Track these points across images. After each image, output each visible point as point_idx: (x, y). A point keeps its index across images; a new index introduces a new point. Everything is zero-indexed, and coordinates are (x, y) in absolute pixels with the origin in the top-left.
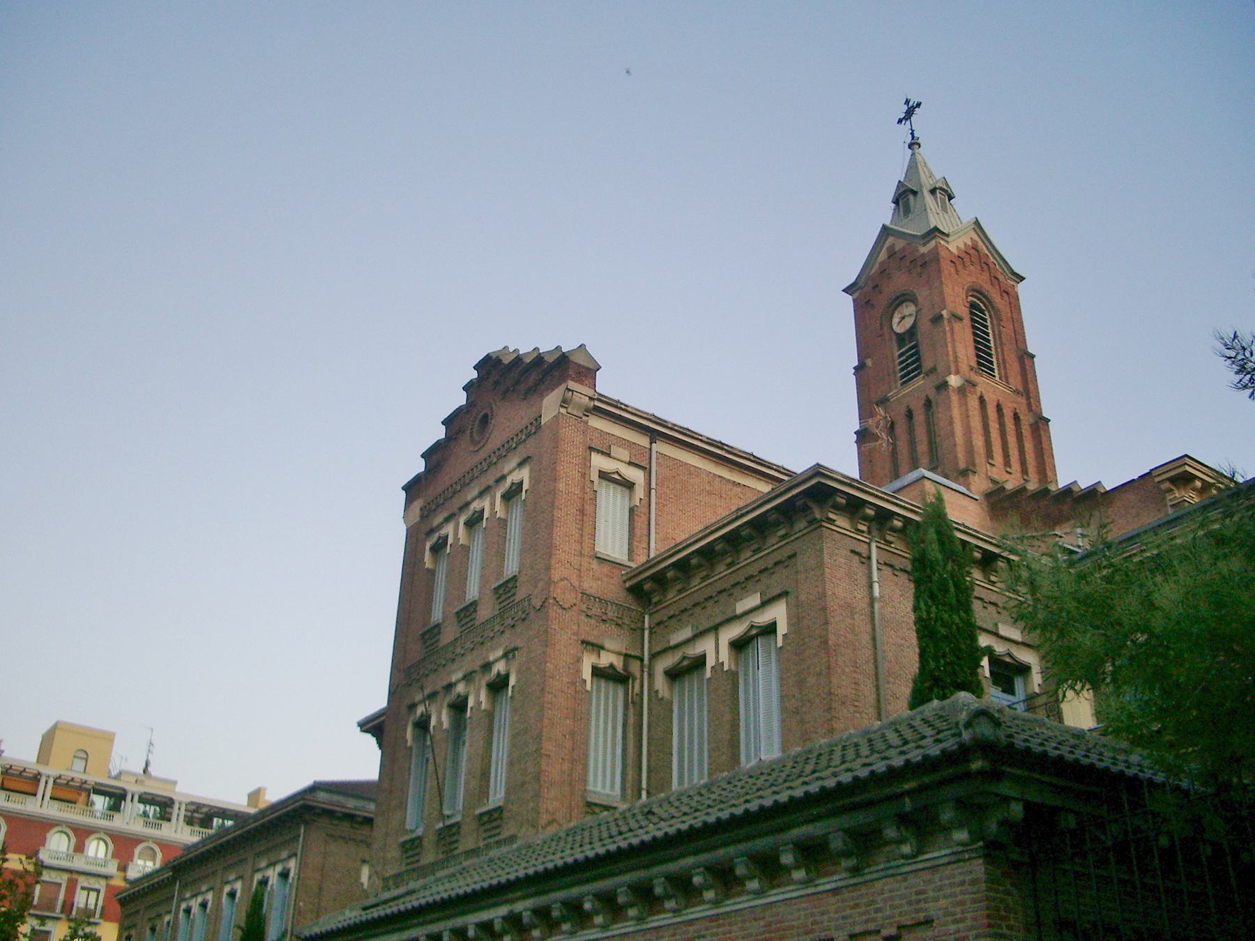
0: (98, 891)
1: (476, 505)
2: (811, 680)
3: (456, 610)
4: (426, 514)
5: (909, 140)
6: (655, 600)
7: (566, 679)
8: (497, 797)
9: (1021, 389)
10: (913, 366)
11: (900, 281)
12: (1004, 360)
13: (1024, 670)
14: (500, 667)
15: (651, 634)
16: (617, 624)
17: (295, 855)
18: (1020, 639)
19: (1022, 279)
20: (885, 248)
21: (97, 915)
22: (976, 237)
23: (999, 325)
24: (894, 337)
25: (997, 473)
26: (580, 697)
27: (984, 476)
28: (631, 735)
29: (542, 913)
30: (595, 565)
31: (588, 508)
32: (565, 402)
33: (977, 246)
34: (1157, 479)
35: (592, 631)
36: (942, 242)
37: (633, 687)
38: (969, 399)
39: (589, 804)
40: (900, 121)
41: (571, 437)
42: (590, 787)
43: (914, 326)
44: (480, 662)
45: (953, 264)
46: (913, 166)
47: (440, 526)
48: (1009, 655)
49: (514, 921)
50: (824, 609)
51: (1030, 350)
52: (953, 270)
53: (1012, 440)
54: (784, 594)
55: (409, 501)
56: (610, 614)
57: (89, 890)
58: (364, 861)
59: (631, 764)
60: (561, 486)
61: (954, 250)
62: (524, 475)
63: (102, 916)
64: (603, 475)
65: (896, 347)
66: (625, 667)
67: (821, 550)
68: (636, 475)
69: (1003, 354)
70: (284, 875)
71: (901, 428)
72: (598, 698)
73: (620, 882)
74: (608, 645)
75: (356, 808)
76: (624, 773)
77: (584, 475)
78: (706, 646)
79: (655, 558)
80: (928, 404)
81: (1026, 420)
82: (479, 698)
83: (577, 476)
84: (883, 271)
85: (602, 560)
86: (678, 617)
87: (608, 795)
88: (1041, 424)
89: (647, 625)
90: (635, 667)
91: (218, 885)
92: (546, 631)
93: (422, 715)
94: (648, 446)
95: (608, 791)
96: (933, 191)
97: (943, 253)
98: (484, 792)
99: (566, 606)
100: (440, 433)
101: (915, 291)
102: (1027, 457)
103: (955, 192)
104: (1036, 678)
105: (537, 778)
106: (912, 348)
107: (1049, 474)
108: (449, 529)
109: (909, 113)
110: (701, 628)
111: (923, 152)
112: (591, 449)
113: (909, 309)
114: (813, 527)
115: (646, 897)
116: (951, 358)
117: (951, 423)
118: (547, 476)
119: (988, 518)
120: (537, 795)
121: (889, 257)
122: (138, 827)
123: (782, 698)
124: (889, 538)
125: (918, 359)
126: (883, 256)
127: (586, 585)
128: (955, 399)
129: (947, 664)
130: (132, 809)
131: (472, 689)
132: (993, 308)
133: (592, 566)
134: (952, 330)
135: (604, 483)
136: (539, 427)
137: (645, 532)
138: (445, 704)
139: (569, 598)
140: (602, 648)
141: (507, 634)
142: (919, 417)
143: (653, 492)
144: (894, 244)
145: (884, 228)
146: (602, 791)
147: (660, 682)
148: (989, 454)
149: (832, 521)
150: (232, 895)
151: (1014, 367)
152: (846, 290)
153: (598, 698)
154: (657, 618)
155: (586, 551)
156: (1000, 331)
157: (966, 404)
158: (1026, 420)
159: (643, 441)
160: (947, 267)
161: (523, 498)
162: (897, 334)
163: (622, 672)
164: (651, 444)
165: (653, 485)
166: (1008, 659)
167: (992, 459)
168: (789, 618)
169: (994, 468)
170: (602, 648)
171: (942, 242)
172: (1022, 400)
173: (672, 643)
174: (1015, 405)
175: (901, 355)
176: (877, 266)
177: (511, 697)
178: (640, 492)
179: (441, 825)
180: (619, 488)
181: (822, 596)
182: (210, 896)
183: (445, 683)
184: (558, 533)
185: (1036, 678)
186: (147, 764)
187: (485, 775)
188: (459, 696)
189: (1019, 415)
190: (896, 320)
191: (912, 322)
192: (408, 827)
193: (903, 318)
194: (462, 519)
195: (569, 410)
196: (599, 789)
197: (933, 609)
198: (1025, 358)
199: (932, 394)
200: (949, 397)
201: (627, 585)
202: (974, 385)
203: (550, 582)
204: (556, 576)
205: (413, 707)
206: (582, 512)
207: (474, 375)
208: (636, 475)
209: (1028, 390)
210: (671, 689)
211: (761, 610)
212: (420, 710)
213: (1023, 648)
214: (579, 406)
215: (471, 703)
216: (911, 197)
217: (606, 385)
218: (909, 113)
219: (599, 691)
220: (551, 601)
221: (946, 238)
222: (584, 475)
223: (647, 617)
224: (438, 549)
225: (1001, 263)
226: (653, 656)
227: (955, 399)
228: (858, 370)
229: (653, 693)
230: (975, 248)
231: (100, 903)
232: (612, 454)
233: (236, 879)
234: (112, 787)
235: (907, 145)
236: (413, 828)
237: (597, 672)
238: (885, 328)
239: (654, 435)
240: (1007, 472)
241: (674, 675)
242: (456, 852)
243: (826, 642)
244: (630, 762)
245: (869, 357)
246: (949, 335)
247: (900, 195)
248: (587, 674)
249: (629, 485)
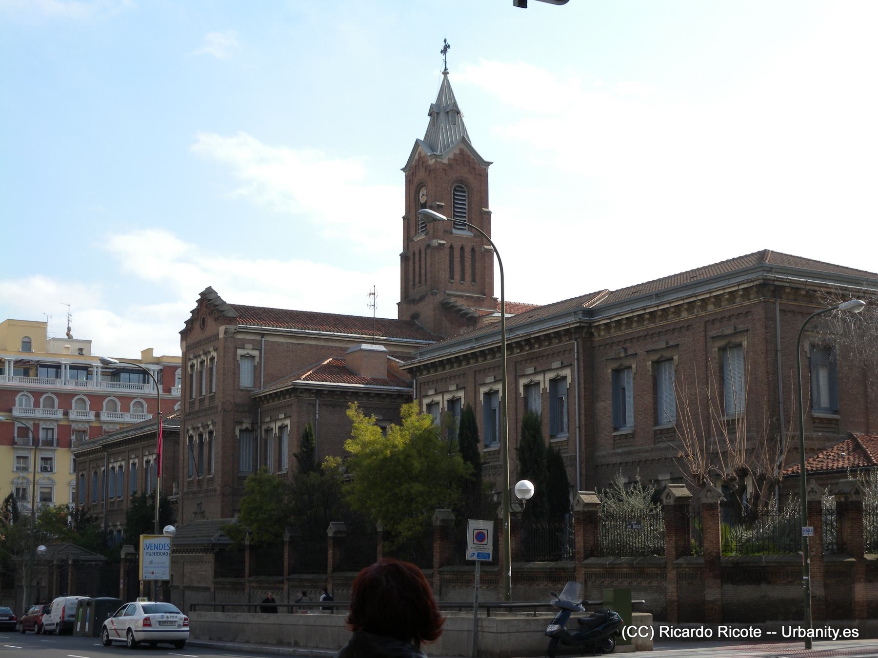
0: (53, 429)
5: (443, 70)
11: (421, 174)
18: (382, 419)
21: (55, 445)
30: (240, 392)
43: (426, 202)
45: (444, 171)
53: (468, 264)
55: (182, 339)
56: (246, 409)
57: (47, 429)
61: (445, 161)
63: (57, 446)
64: (242, 356)
66: (252, 427)
68: (256, 353)
85: (242, 390)
91: (127, 458)
95: (247, 470)
109: (444, 51)
122: (70, 387)
126: (417, 157)
130: (66, 373)
136: (218, 338)
143: (263, 358)
150: (134, 464)
152: (401, 170)
159: (258, 338)
165: (263, 355)
169: (454, 284)
178: (257, 360)
182: (123, 463)
186: (69, 329)
189: (475, 249)
190: (421, 195)
194: (199, 361)
208: (256, 353)
218: (444, 51)
221: (441, 157)
231: (55, 436)
232: (246, 347)
233: (135, 458)
234: (51, 362)
235: (441, 72)
240: (462, 284)
248: (237, 433)
249: (253, 357)
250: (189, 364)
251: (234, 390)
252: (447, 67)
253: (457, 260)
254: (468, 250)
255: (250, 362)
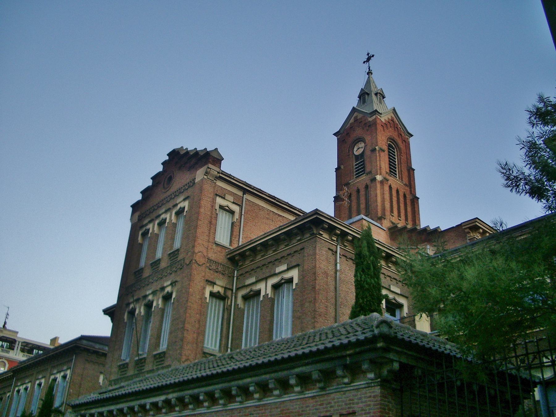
1: (163, 216)
2: (307, 305)
3: (151, 262)
4: (141, 219)
5: (367, 71)
6: (240, 264)
7: (198, 297)
8: (163, 347)
9: (408, 184)
10: (361, 169)
12: (401, 170)
13: (400, 306)
14: (169, 289)
15: (237, 279)
16: (223, 274)
17: (70, 368)
19: (412, 136)
20: (353, 117)
22: (393, 116)
23: (400, 155)
24: (354, 156)
25: (395, 219)
26: (204, 305)
27: (389, 220)
28: (225, 323)
29: (181, 400)
31: (213, 221)
32: (207, 173)
33: (393, 119)
34: (464, 227)
35: (210, 275)
36: (378, 116)
37: (227, 303)
38: (385, 186)
39: (204, 353)
40: (364, 62)
41: (208, 188)
42: (205, 345)
44: (159, 286)
46: (368, 82)
47: (146, 225)
48: (395, 299)
49: (167, 402)
50: (315, 273)
51: (413, 167)
52: (382, 129)
53: (402, 205)
54: (298, 265)
56: (220, 269)
58: (101, 373)
59: (224, 336)
60: (202, 210)
61: (383, 120)
62: (186, 204)
64: (221, 207)
65: (354, 162)
66: (225, 292)
67: (315, 247)
69: (401, 168)
70: (64, 377)
71: (354, 198)
72: (212, 306)
73: (217, 388)
74: (217, 282)
75: (99, 349)
76: (221, 340)
77: (212, 206)
78: (261, 286)
79: (242, 245)
80: (367, 187)
81: (409, 197)
82: (158, 303)
83: (210, 207)
84: (351, 128)
85: (217, 245)
86: (249, 273)
87: (213, 350)
88: (415, 200)
89: (235, 275)
90: (229, 293)
92: (191, 275)
93: (132, 308)
94: (242, 196)
95: (213, 348)
96: (376, 94)
97: (378, 121)
98: (157, 345)
99: (200, 264)
100: (150, 183)
101: (365, 137)
102: (408, 214)
103: (386, 94)
104: (406, 310)
105: (182, 340)
106: (361, 162)
107: (417, 221)
108: (150, 226)
109: (369, 59)
110: (260, 278)
111: (374, 77)
112: (217, 195)
113: (362, 145)
114: (312, 237)
115: (228, 395)
116: (378, 168)
117: (376, 196)
118: (196, 206)
119: (389, 239)
120: (182, 347)
121: (354, 121)
123: (294, 311)
124: (345, 244)
125: (364, 167)
126: (352, 120)
127: (210, 255)
128: (378, 185)
129: (367, 300)
131: (155, 298)
132: (398, 147)
133: (213, 247)
134: (380, 155)
135: (221, 211)
136: (194, 183)
137: (238, 234)
138: (143, 304)
139: (202, 261)
140: (215, 284)
141: (173, 275)
142: (362, 192)
143: (243, 216)
144: (357, 116)
145: (354, 108)
146: (211, 347)
147: (240, 301)
148: (392, 211)
149: (321, 235)
151: (405, 174)
152: (333, 134)
153: (212, 306)
154: (241, 272)
155: (211, 240)
156: (400, 158)
157: (383, 188)
158: (409, 197)
159: (240, 193)
160: (379, 128)
161: (185, 214)
162: (355, 155)
163: (223, 295)
164: (243, 195)
165: (243, 213)
166: (394, 301)
167: (393, 213)
168: (299, 277)
169: (393, 217)
170: (215, 284)
171: (378, 116)
172: (408, 189)
173: (246, 284)
174: (405, 191)
175: (356, 165)
176: (349, 125)
177: (173, 303)
178: (237, 216)
179: (137, 358)
180: (228, 213)
181: (315, 267)
183: (143, 295)
184: (199, 231)
185: (406, 310)
187: (159, 337)
188: (149, 301)
190: (355, 149)
191: (363, 150)
192: (122, 358)
193: (359, 148)
194: (157, 222)
195: (208, 177)
196: (209, 346)
197: (363, 276)
198: (411, 171)
199: (369, 183)
200: (376, 185)
201: (228, 256)
202: (387, 180)
203: (194, 253)
204: (196, 250)
205: (128, 304)
206: (210, 223)
207: (167, 158)
209: (411, 184)
210: (244, 304)
211: (287, 272)
212: (132, 306)
213: (401, 296)
214: (212, 175)
215: (155, 304)
216: (366, 96)
217: (225, 167)
218: (369, 59)
219: (212, 303)
220: (194, 261)
222: (212, 206)
223: (236, 272)
224: (145, 234)
225: (403, 128)
226: (238, 289)
227: (378, 185)
228: (337, 170)
229: (236, 305)
230: (392, 120)
236: (125, 359)
237: (212, 294)
238: (351, 152)
239: (245, 191)
240: (399, 219)
241: (246, 298)
242: (143, 371)
243: (314, 288)
244: (224, 335)
245: (342, 164)
246: (378, 158)
247: (362, 94)
248: (207, 295)
249: (232, 212)
250: (140, 233)
251: (209, 241)
252: (371, 69)
253: (395, 199)
254: (401, 194)
255: (227, 217)
